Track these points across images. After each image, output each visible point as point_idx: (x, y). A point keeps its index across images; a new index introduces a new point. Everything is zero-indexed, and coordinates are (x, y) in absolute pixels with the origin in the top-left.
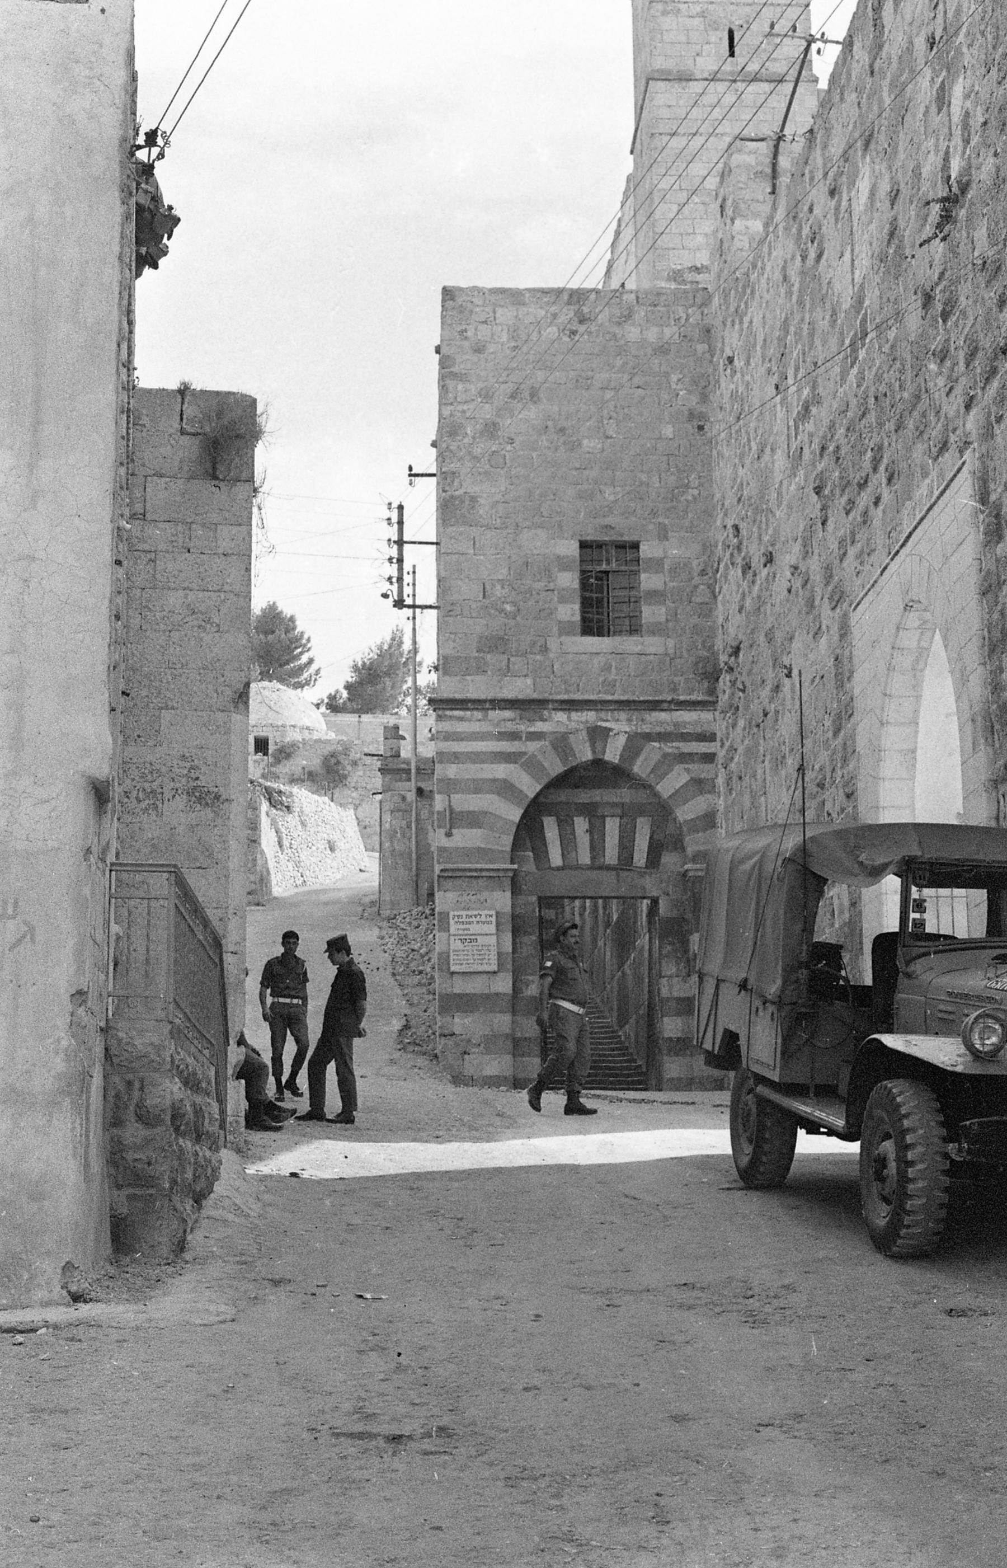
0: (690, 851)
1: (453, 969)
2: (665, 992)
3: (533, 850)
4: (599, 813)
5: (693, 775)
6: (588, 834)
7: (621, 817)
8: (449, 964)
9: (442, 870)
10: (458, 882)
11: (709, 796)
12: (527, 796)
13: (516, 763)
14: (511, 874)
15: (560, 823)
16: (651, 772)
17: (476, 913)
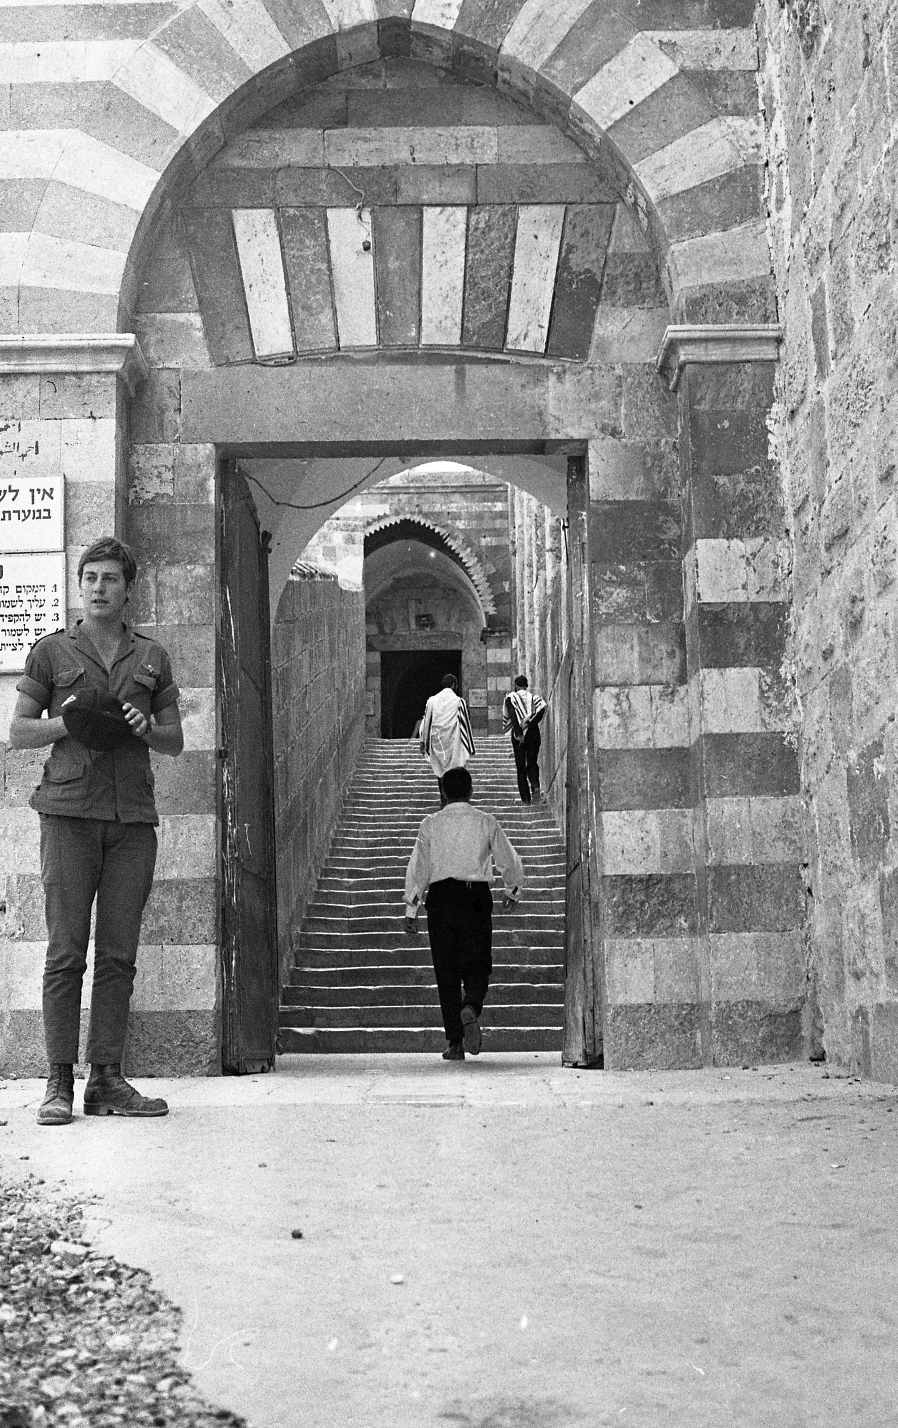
0: (678, 297)
4: (408, 193)
5: (690, 65)
6: (369, 258)
7: (472, 207)
11: (736, 122)
12: (175, 133)
13: (140, 34)
15: (284, 226)
16: (555, 56)
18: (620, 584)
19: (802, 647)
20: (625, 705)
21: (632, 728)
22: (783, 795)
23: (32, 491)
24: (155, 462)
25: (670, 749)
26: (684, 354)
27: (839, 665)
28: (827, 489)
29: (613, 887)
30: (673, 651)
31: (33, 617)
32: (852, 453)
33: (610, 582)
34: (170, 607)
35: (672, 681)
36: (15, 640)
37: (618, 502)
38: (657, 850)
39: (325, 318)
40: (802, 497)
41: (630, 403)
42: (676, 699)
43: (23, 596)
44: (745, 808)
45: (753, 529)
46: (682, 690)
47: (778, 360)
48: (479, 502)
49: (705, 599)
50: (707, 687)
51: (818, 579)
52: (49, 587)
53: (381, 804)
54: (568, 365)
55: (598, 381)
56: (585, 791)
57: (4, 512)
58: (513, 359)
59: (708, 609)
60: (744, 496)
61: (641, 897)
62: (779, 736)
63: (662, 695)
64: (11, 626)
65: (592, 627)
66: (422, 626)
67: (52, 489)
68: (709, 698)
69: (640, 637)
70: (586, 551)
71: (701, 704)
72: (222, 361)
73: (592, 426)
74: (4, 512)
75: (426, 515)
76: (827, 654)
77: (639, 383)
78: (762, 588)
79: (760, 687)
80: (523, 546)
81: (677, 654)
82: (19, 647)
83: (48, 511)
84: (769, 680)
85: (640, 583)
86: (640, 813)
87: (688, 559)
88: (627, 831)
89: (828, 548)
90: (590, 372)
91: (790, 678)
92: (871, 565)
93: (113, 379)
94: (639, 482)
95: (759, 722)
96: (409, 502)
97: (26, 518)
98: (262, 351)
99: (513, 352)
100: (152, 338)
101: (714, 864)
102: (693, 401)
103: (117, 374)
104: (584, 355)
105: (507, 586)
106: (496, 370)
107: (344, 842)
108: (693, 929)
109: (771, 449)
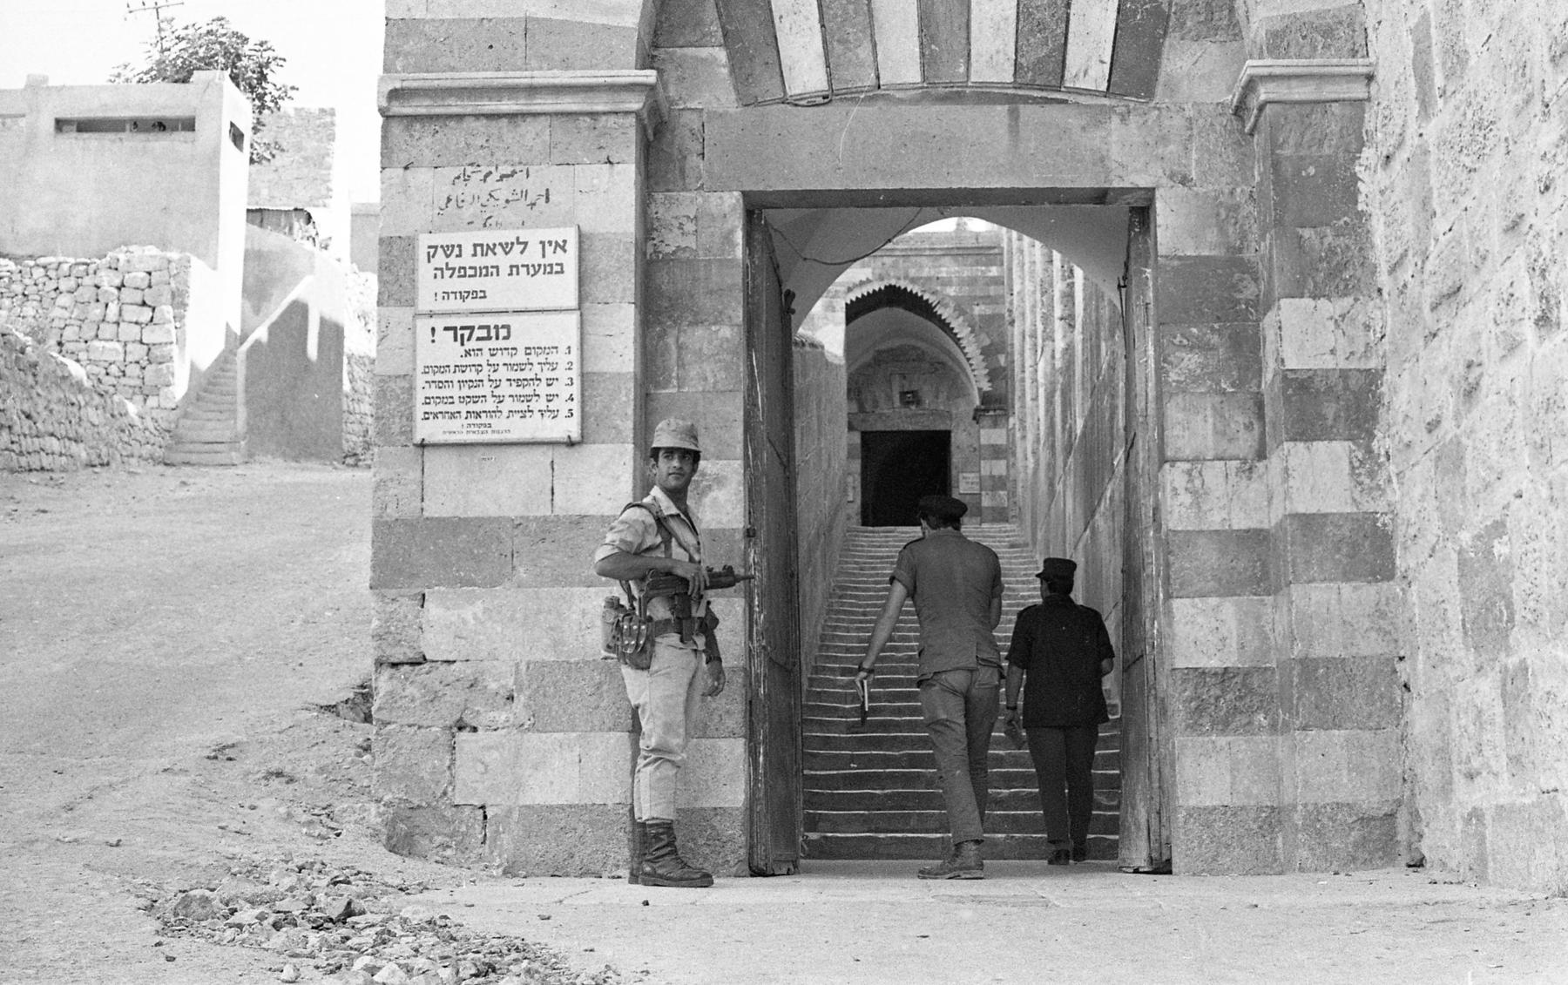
1: (426, 430)
2: (1178, 514)
3: (728, 39)
8: (411, 418)
9: (394, 95)
10: (455, 135)
14: (635, 103)
17: (508, 236)
18: (1192, 348)
19: (1400, 418)
20: (1198, 483)
21: (1205, 507)
22: (1377, 581)
23: (542, 243)
24: (675, 211)
25: (1248, 531)
26: (1264, 93)
27: (1448, 437)
28: (1433, 242)
29: (1184, 681)
30: (1251, 423)
31: (544, 382)
32: (1466, 201)
33: (1181, 346)
34: (693, 372)
35: (1250, 457)
36: (524, 407)
37: (1189, 257)
38: (1233, 643)
39: (864, 52)
40: (1400, 251)
41: (1203, 149)
42: (1254, 476)
43: (533, 359)
44: (1335, 596)
45: (1342, 287)
46: (1261, 465)
47: (1369, 99)
48: (971, 265)
49: (1290, 365)
50: (1292, 462)
51: (1421, 343)
52: (562, 349)
53: (871, 597)
54: (1132, 105)
55: (1167, 122)
56: (1150, 576)
57: (511, 267)
58: (1071, 98)
59: (1291, 376)
60: (1332, 251)
61: (1215, 691)
62: (1372, 517)
63: (1238, 470)
64: (520, 391)
65: (1159, 398)
66: (906, 403)
67: (565, 241)
68: (1295, 474)
69: (1214, 408)
70: (1151, 312)
71: (1286, 480)
72: (749, 101)
73: (1160, 172)
74: (511, 267)
75: (913, 281)
76: (1432, 426)
77: (1212, 125)
78: (1352, 353)
79: (1351, 463)
80: (1023, 314)
81: (1256, 426)
82: (528, 414)
83: (561, 265)
84: (1360, 457)
85: (1213, 348)
86: (1213, 601)
87: (1269, 321)
88: (1200, 620)
89: (1434, 308)
90: (1157, 112)
91: (1383, 452)
92: (1491, 325)
93: (632, 120)
94: (1212, 235)
95: (1349, 501)
96: (895, 266)
97: (536, 273)
98: (795, 88)
99: (1071, 91)
100: (672, 75)
101: (1301, 656)
102: (1274, 144)
103: (637, 114)
104: (1150, 94)
105: (1002, 359)
106: (1052, 112)
107: (834, 637)
108: (1273, 727)
109: (1361, 198)
